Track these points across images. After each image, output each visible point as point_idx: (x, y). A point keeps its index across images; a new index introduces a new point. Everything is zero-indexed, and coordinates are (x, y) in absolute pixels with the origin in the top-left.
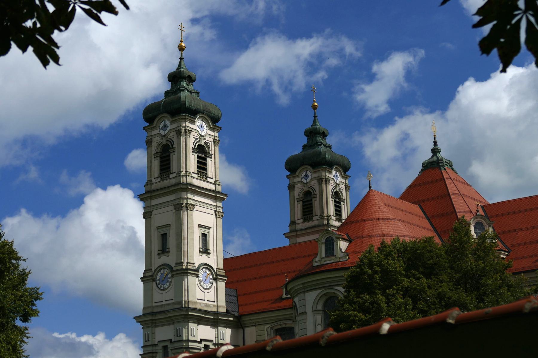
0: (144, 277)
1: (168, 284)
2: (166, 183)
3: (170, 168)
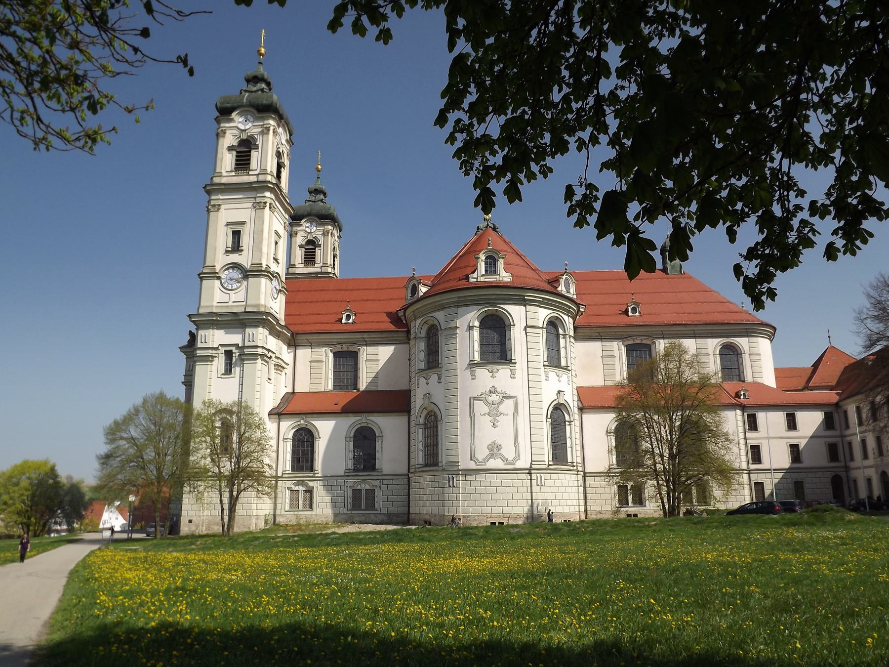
2: (245, 179)
3: (249, 164)
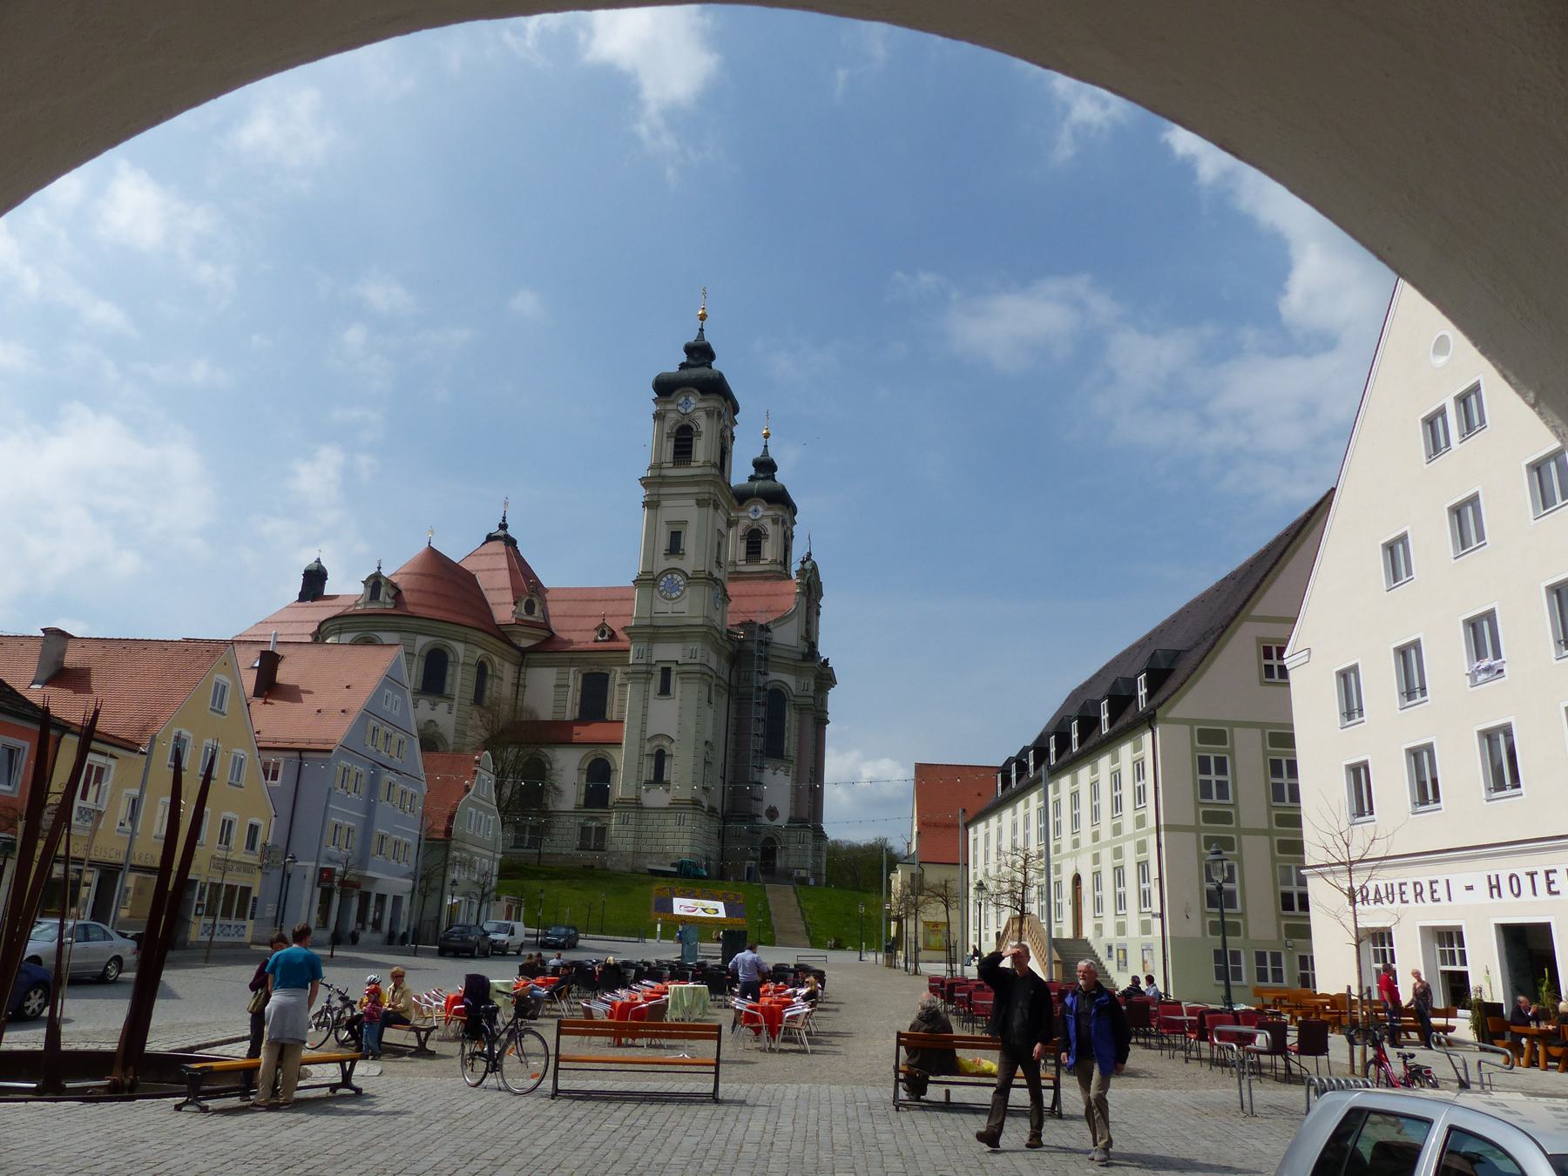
0: (636, 580)
1: (678, 593)
3: (691, 452)
